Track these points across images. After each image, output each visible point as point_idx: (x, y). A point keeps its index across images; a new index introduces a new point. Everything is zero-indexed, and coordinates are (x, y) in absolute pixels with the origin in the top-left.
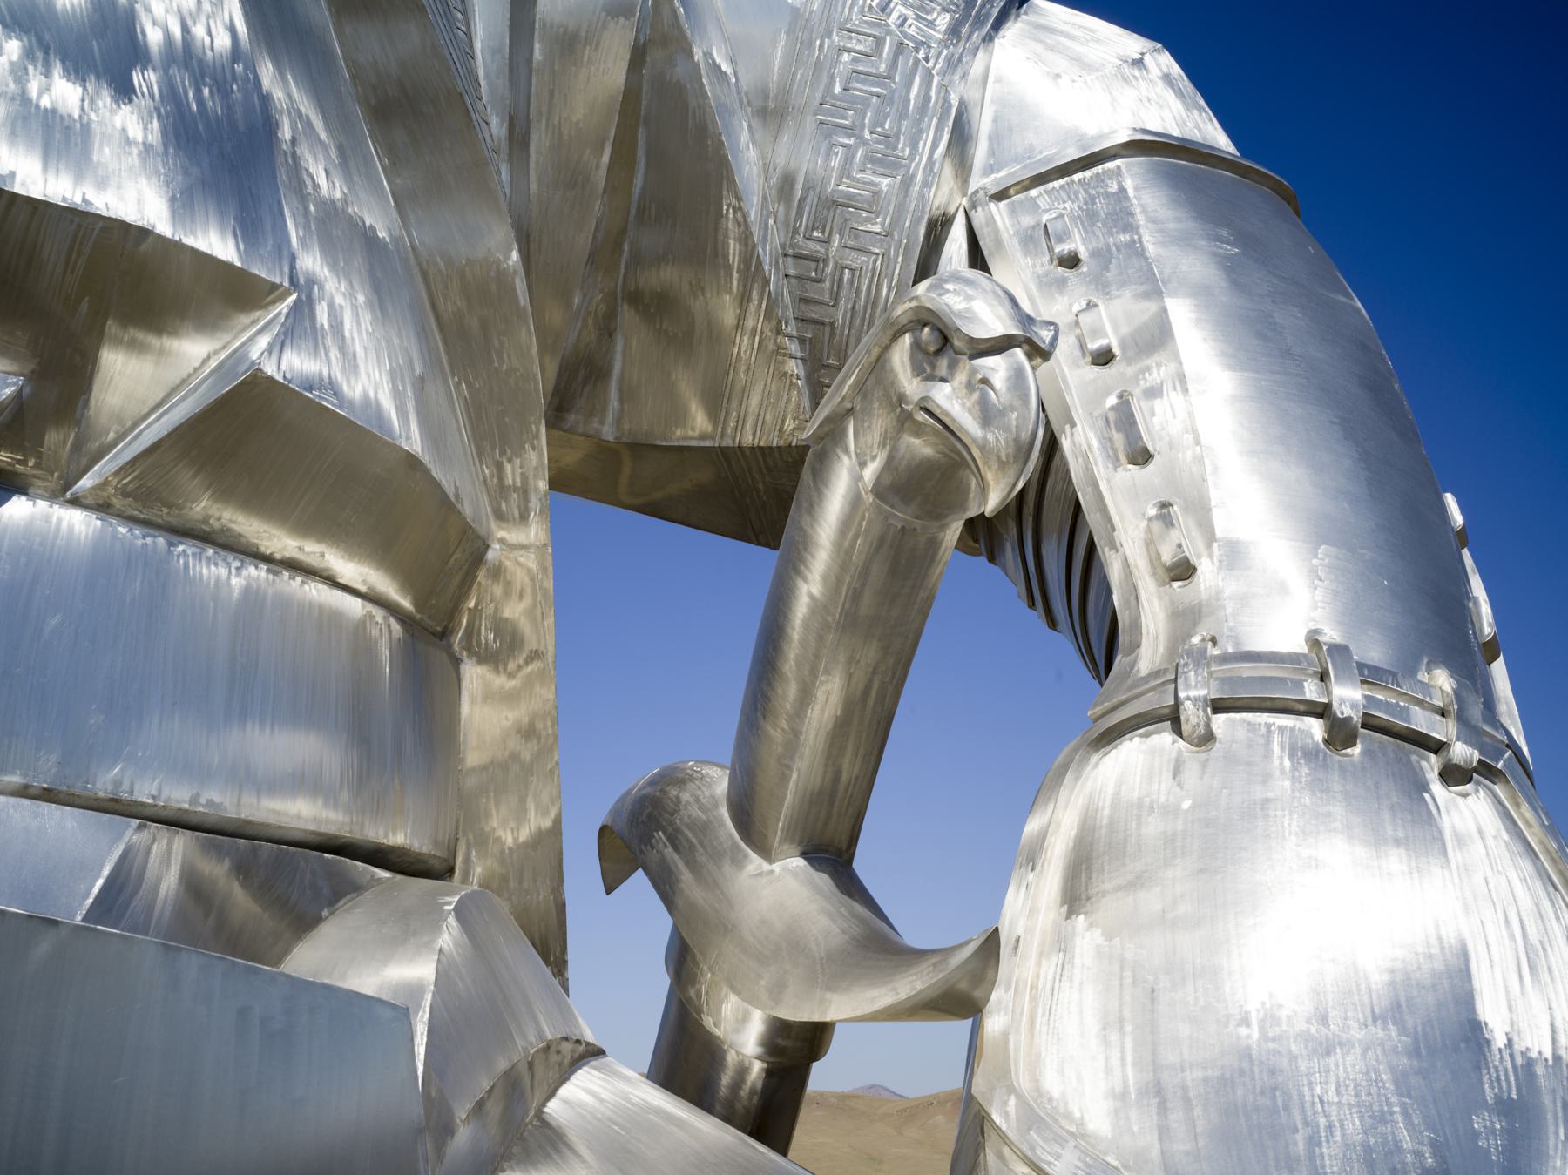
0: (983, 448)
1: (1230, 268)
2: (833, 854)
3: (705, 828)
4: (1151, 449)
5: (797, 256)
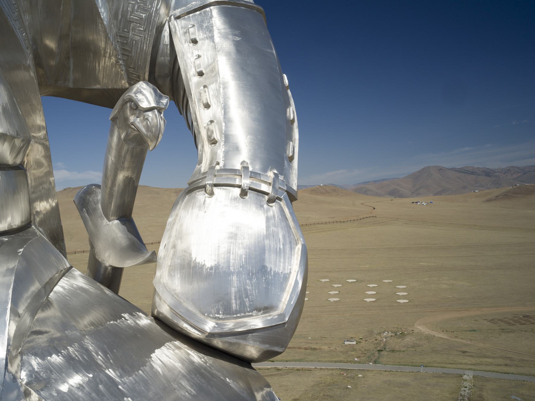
0: (147, 136)
1: (237, 45)
2: (125, 217)
3: (95, 210)
4: (209, 103)
5: (120, 36)
